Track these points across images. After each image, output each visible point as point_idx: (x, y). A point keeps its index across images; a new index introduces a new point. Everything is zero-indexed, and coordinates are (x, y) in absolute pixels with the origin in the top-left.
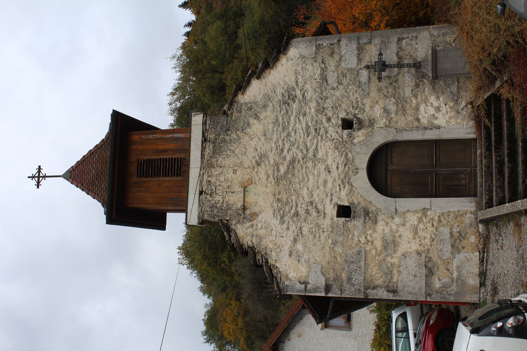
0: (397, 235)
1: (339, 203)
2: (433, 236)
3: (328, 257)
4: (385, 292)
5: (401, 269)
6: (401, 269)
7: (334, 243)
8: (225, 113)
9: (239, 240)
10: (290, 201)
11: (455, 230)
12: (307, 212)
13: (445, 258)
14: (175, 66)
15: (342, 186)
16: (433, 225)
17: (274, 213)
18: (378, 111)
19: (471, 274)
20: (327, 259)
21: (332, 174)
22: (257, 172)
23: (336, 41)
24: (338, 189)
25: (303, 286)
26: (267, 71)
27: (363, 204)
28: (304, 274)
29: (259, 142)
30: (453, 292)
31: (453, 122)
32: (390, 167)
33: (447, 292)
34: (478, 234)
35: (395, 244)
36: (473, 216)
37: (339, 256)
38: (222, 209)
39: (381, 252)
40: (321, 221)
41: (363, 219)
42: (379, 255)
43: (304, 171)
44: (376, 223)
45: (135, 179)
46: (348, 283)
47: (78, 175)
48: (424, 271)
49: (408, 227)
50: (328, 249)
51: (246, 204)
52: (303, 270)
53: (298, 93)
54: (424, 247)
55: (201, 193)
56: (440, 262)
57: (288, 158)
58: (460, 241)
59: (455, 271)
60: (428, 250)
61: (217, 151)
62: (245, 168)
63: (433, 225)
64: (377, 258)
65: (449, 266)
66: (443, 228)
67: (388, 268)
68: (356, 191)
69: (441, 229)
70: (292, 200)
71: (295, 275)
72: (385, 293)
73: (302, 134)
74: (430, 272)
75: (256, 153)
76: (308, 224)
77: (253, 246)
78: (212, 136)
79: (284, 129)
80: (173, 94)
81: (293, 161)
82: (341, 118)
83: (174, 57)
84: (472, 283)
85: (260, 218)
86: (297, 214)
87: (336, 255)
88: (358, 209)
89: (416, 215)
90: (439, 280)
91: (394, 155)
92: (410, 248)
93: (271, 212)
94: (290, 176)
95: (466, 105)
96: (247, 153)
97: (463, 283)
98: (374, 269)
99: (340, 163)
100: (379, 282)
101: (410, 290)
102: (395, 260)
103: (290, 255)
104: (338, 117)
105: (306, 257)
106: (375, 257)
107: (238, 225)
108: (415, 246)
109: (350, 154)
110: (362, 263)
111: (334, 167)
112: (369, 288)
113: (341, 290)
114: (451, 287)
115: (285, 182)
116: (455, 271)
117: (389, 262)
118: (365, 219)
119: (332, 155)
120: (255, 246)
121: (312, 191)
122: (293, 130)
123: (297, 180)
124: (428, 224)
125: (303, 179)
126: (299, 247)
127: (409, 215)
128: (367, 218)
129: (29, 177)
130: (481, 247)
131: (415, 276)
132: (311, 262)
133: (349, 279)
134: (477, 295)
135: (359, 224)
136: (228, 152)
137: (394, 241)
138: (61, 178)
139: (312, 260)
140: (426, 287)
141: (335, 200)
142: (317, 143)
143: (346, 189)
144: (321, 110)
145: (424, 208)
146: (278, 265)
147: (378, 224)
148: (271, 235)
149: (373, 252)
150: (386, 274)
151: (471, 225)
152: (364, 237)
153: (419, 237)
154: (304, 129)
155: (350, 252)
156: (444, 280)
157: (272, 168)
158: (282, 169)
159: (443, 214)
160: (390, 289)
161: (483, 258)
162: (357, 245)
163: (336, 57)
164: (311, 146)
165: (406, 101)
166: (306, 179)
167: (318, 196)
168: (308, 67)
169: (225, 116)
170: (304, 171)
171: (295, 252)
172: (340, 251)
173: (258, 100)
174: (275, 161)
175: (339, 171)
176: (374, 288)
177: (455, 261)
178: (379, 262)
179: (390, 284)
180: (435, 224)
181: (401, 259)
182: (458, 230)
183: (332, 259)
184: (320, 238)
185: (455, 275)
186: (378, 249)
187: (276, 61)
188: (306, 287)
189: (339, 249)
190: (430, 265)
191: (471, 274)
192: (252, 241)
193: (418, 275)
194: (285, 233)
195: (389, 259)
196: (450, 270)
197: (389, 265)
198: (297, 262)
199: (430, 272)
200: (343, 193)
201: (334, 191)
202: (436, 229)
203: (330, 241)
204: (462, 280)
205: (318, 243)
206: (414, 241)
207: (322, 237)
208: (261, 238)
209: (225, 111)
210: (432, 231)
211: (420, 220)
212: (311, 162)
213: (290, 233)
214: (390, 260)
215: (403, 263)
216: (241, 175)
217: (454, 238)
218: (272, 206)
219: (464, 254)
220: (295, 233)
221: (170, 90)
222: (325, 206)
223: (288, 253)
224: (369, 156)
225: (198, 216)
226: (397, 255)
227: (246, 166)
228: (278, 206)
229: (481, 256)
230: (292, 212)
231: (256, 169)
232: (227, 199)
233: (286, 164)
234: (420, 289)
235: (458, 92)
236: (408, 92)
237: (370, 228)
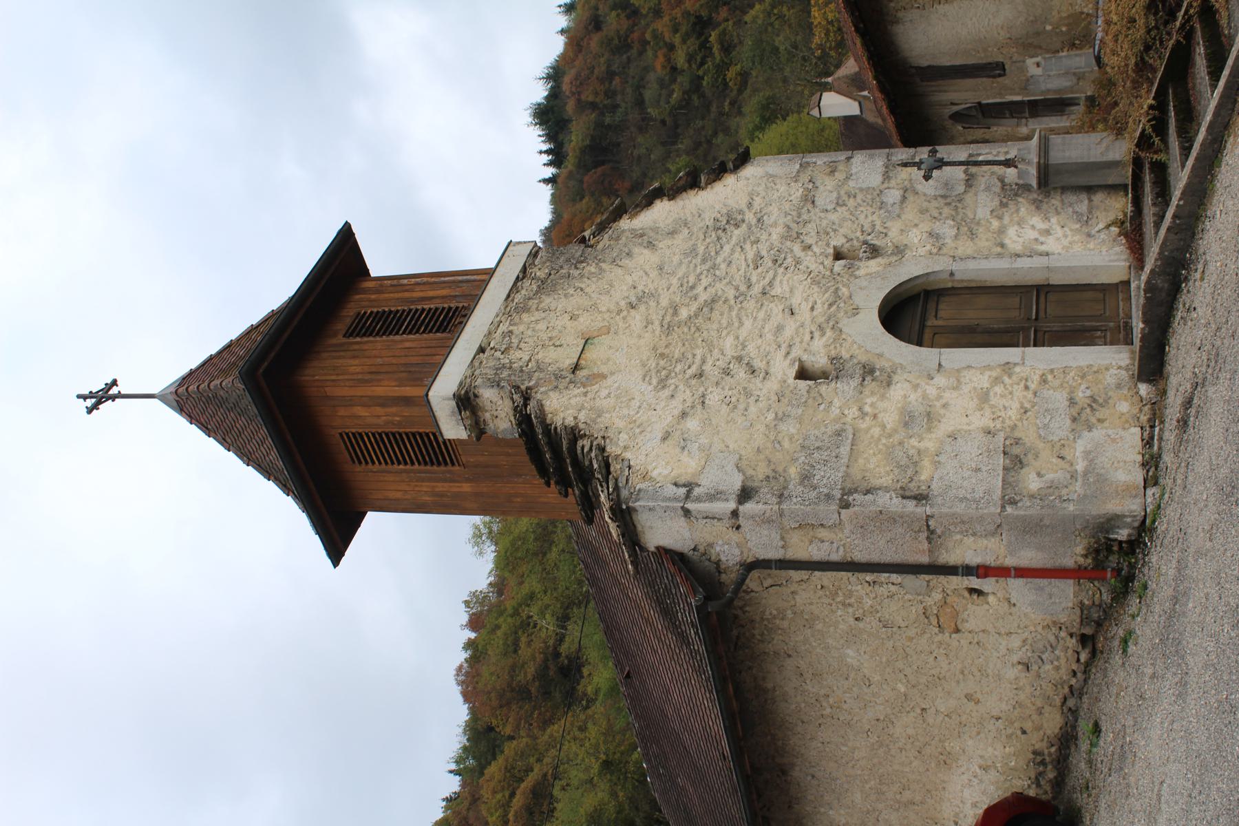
0: (938, 404)
1: (805, 357)
2: (1027, 405)
3: (759, 440)
4: (895, 500)
5: (942, 458)
6: (942, 458)
7: (780, 418)
8: (583, 240)
10: (690, 356)
11: (1081, 395)
12: (727, 372)
13: (1056, 439)
15: (817, 334)
16: (1027, 388)
17: (645, 376)
18: (915, 237)
21: (797, 317)
23: (843, 158)
24: (807, 337)
25: (683, 491)
26: (692, 193)
27: (863, 358)
28: (690, 471)
29: (645, 278)
30: (1075, 497)
31: (1077, 248)
33: (1060, 497)
34: (1136, 399)
35: (931, 418)
36: (1124, 372)
37: (786, 439)
38: (522, 371)
39: (895, 431)
40: (756, 384)
41: (857, 380)
42: (890, 436)
43: (734, 313)
44: (889, 384)
45: (340, 339)
46: (801, 483)
47: (195, 398)
48: (1001, 461)
49: (966, 391)
50: (762, 428)
51: (582, 362)
52: (688, 466)
53: (750, 217)
54: (1003, 422)
55: (482, 350)
57: (704, 297)
58: (1093, 409)
59: (1080, 460)
60: (1014, 428)
61: (544, 286)
63: (1027, 388)
64: (884, 441)
65: (1066, 452)
67: (909, 458)
69: (1048, 393)
70: (694, 355)
71: (666, 472)
72: (896, 500)
73: (744, 266)
74: (1015, 462)
75: (633, 291)
76: (723, 389)
77: (576, 426)
78: (541, 274)
79: (704, 261)
82: (835, 248)
85: (609, 381)
86: (700, 375)
87: (780, 438)
88: (848, 366)
89: (988, 373)
90: (1039, 475)
91: (941, 306)
94: (700, 320)
95: (1108, 227)
96: (612, 292)
97: (1102, 480)
98: (874, 460)
99: (819, 302)
100: (886, 481)
101: (962, 493)
102: (929, 444)
103: (664, 439)
104: (828, 245)
105: (704, 440)
106: (879, 439)
107: (551, 394)
108: (980, 421)
109: (844, 290)
110: (845, 450)
111: (806, 307)
112: (856, 491)
115: (686, 330)
116: (1080, 460)
117: (913, 447)
119: (804, 291)
120: (581, 426)
122: (724, 261)
123: (715, 326)
126: (692, 424)
127: (967, 375)
128: (868, 378)
129: (79, 397)
130: (1144, 418)
131: (978, 470)
133: (805, 478)
134: (1139, 500)
135: (846, 388)
136: (571, 291)
137: (929, 414)
138: (156, 400)
140: (1003, 488)
141: (796, 352)
142: (775, 276)
143: (824, 339)
144: (793, 235)
146: (628, 455)
147: (893, 387)
148: (628, 407)
149: (876, 431)
150: (903, 468)
151: (1119, 386)
152: (855, 409)
153: (992, 407)
154: (750, 261)
156: (1050, 476)
158: (684, 313)
159: (1052, 371)
160: (908, 494)
161: (1152, 438)
162: (836, 420)
163: (840, 176)
164: (758, 281)
165: (978, 224)
166: (736, 324)
168: (778, 186)
169: (583, 246)
170: (734, 313)
171: (679, 432)
172: (793, 431)
173: (661, 225)
175: (815, 313)
176: (868, 492)
177: (1080, 442)
178: (888, 448)
179: (912, 485)
180: (1033, 386)
181: (942, 443)
182: (1088, 393)
183: (769, 445)
185: (1080, 466)
186: (888, 427)
188: (689, 492)
189: (790, 428)
190: (1016, 450)
191: (1122, 464)
192: (575, 418)
193: (984, 469)
194: (663, 404)
195: (914, 442)
197: (911, 452)
198: (678, 450)
199: (1015, 462)
200: (818, 343)
201: (798, 340)
202: (1035, 394)
203: (771, 416)
205: (740, 420)
206: (978, 414)
207: (753, 409)
209: (584, 237)
210: (1025, 397)
211: (997, 380)
212: (753, 301)
213: (674, 403)
214: (916, 444)
215: (948, 448)
216: (586, 322)
217: (1077, 408)
218: (644, 365)
219: (1104, 431)
223: (660, 435)
225: (461, 384)
226: (933, 436)
227: (604, 309)
229: (1146, 434)
230: (694, 369)
231: (625, 313)
232: (540, 356)
233: (694, 307)
234: (988, 492)
235: (1090, 212)
236: (983, 212)
237: (873, 393)
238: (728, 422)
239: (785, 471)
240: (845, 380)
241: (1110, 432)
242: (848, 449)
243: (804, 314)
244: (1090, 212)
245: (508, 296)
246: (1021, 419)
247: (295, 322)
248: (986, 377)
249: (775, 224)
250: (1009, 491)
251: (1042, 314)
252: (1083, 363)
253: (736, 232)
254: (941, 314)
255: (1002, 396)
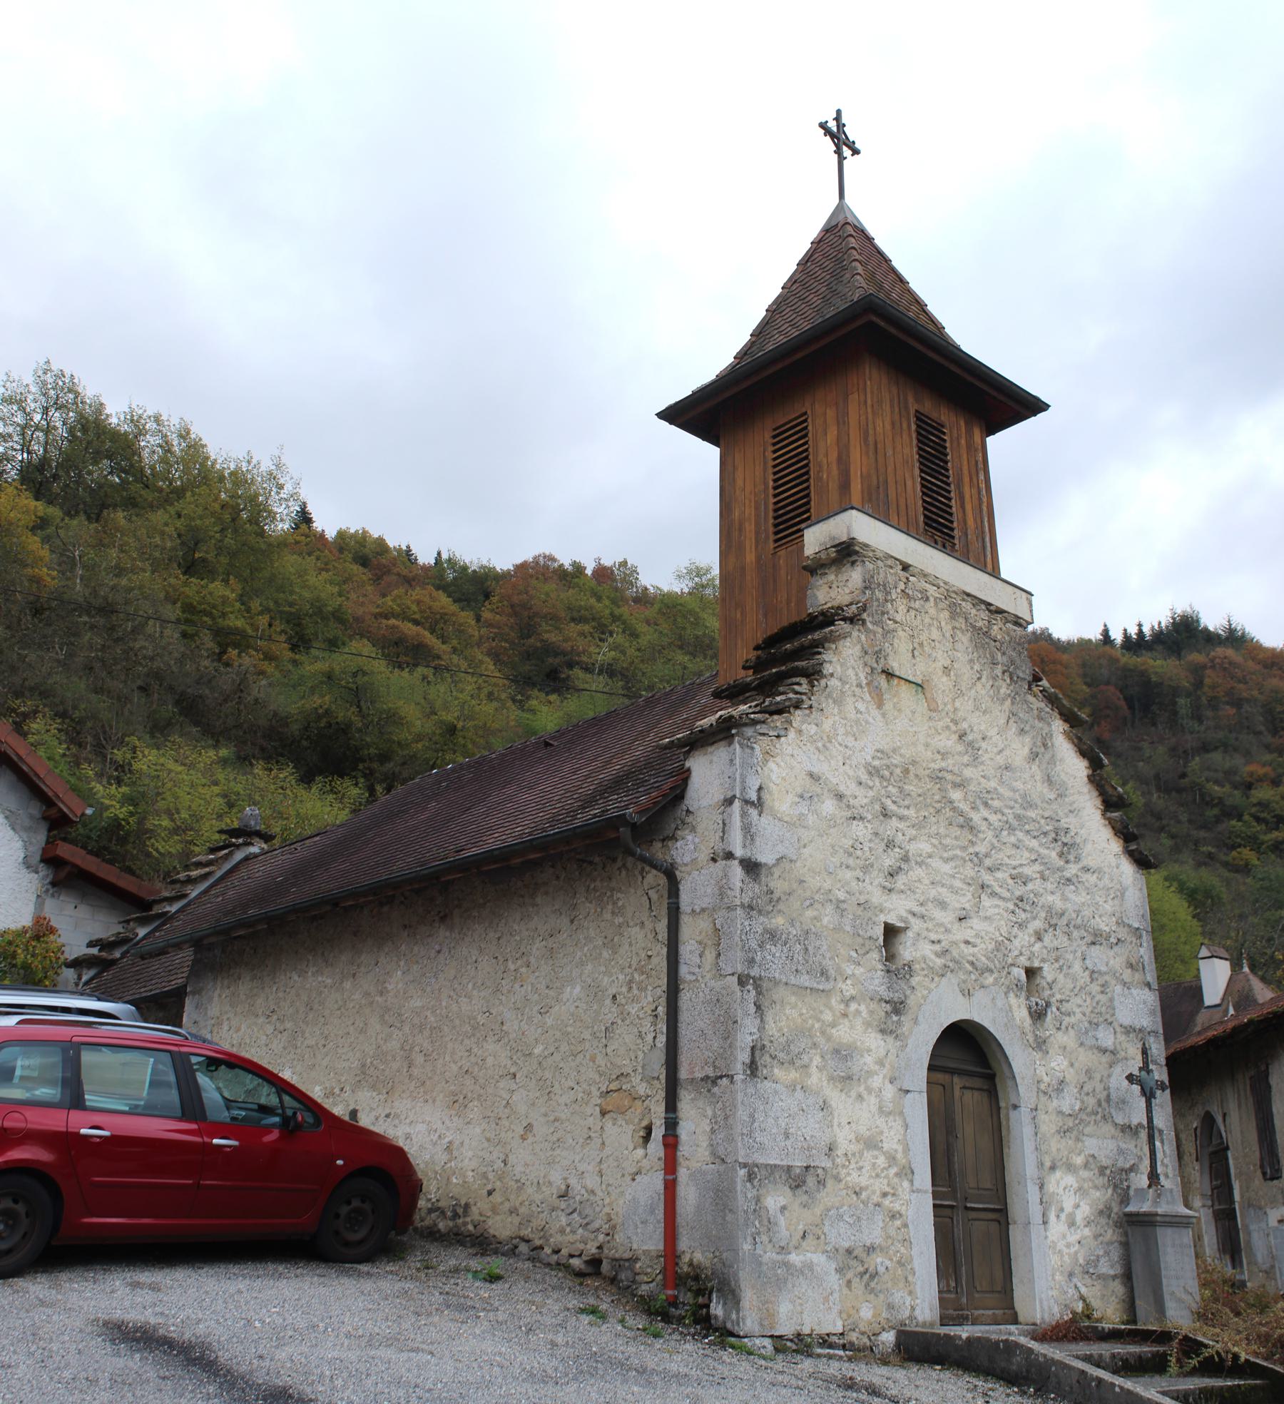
1: (910, 934)
2: (864, 1195)
3: (814, 882)
4: (749, 1039)
5: (799, 1094)
6: (799, 1094)
7: (839, 906)
8: (1037, 679)
9: (834, 642)
10: (906, 803)
11: (879, 1260)
12: (890, 844)
14: (254, 461)
15: (937, 948)
16: (885, 1195)
17: (882, 752)
18: (1058, 1063)
19: (799, 1308)
20: (807, 878)
21: (957, 925)
22: (948, 727)
23: (1149, 978)
24: (934, 937)
25: (754, 797)
26: (1098, 802)
27: (912, 1001)
28: (777, 804)
29: (995, 750)
30: (759, 1251)
31: (1055, 1260)
32: (958, 1082)
33: (758, 1234)
34: (877, 1328)
36: (907, 1313)
37: (815, 913)
38: (883, 613)
39: (829, 1039)
41: (886, 995)
42: (823, 1033)
43: (958, 852)
44: (883, 1031)
46: (766, 931)
47: (841, 244)
48: (799, 1163)
50: (827, 886)
51: (896, 681)
52: (782, 802)
53: (1072, 870)
54: (843, 1166)
55: (906, 567)
56: (818, 1211)
57: (976, 817)
58: (862, 1274)
59: (801, 1258)
60: (837, 1179)
61: (981, 636)
62: (954, 700)
63: (885, 1195)
64: (817, 1026)
66: (881, 1224)
68: (933, 986)
69: (879, 1218)
70: (908, 807)
73: (1014, 863)
74: (798, 1179)
76: (870, 841)
79: (1018, 817)
80: (184, 434)
81: (968, 826)
82: (1040, 969)
83: (278, 466)
84: (781, 1310)
85: (875, 712)
86: (885, 814)
87: (816, 906)
88: (902, 984)
89: (900, 1148)
90: (783, 1208)
91: (976, 1093)
92: (839, 1125)
93: (884, 744)
94: (949, 814)
95: (1083, 1298)
96: (978, 713)
97: (780, 1284)
98: (795, 1013)
99: (976, 950)
100: (771, 1028)
101: (760, 1116)
102: (815, 1078)
103: (811, 775)
104: (1043, 960)
105: (811, 819)
107: (859, 647)
108: (844, 1140)
110: (805, 980)
111: (969, 934)
112: (759, 993)
113: (751, 907)
114: (770, 1246)
115: (937, 797)
116: (801, 1258)
117: (811, 1060)
118: (887, 1002)
119: (987, 933)
120: (823, 682)
121: (927, 865)
122: (1019, 841)
123: (942, 830)
124: (886, 1181)
125: (945, 848)
126: (829, 806)
127: (897, 1124)
128: (888, 1007)
129: (839, 112)
130: (853, 1337)
131: (787, 1135)
132: (801, 831)
133: (772, 935)
134: (757, 1330)
135: (877, 982)
136: (977, 667)
137: (850, 1078)
138: (837, 201)
139: (805, 835)
140: (767, 1165)
141: (916, 925)
142: (1004, 899)
143: (933, 957)
144: (1053, 920)
145: (913, 1173)
146: (792, 734)
147: (879, 1036)
148: (847, 734)
149: (828, 1017)
150: (786, 1047)
151: (890, 1307)
152: (853, 992)
154: (1020, 870)
155: (825, 947)
156: (782, 1222)
157: (956, 770)
158: (956, 795)
159: (906, 1225)
160: (757, 1053)
161: (831, 1346)
162: (839, 970)
163: (1127, 975)
164: (997, 880)
165: (1078, 1139)
166: (945, 855)
167: (919, 881)
168: (1110, 902)
169: (1030, 678)
170: (958, 852)
171: (819, 791)
172: (825, 920)
174: (969, 780)
175: (962, 946)
176: (758, 1007)
178: (810, 1030)
179: (767, 1058)
180: (887, 1202)
181: (817, 1093)
182: (881, 1270)
183: (808, 893)
184: (847, 867)
185: (794, 1258)
186: (834, 1031)
187: (1113, 828)
189: (828, 917)
190: (811, 1181)
191: (799, 1308)
192: (832, 675)
193: (788, 1143)
194: (851, 773)
195: (817, 1060)
196: (804, 1244)
197: (805, 1058)
198: (799, 790)
199: (798, 1179)
200: (927, 950)
201: (930, 926)
202: (878, 1205)
203: (841, 895)
204: (786, 1281)
206: (852, 1136)
207: (848, 875)
208: (839, 702)
209: (1040, 680)
210: (874, 1192)
211: (892, 1159)
212: (972, 873)
213: (853, 786)
214: (815, 1063)
215: (811, 1101)
216: (942, 683)
218: (894, 750)
219: (836, 1287)
220: (852, 802)
221: (197, 431)
222: (903, 896)
223: (815, 770)
224: (991, 1030)
225: (867, 546)
226: (825, 1083)
227: (957, 704)
228: (896, 766)
229: (835, 1339)
230: (893, 807)
231: (954, 728)
232: (901, 633)
233: (964, 807)
235: (1099, 1277)
236: (1091, 1145)
237: (871, 1012)
238: (833, 847)
239: (779, 911)
240: (886, 980)
241: (836, 1295)
242: (807, 984)
243: (960, 933)
244: (1099, 1277)
245: (968, 595)
246: (847, 1188)
247: (931, 354)
248: (895, 1146)
249: (1065, 899)
250: (764, 1172)
251: (973, 1215)
252: (916, 1264)
253: (1054, 854)
254: (968, 1094)
255: (874, 1164)
